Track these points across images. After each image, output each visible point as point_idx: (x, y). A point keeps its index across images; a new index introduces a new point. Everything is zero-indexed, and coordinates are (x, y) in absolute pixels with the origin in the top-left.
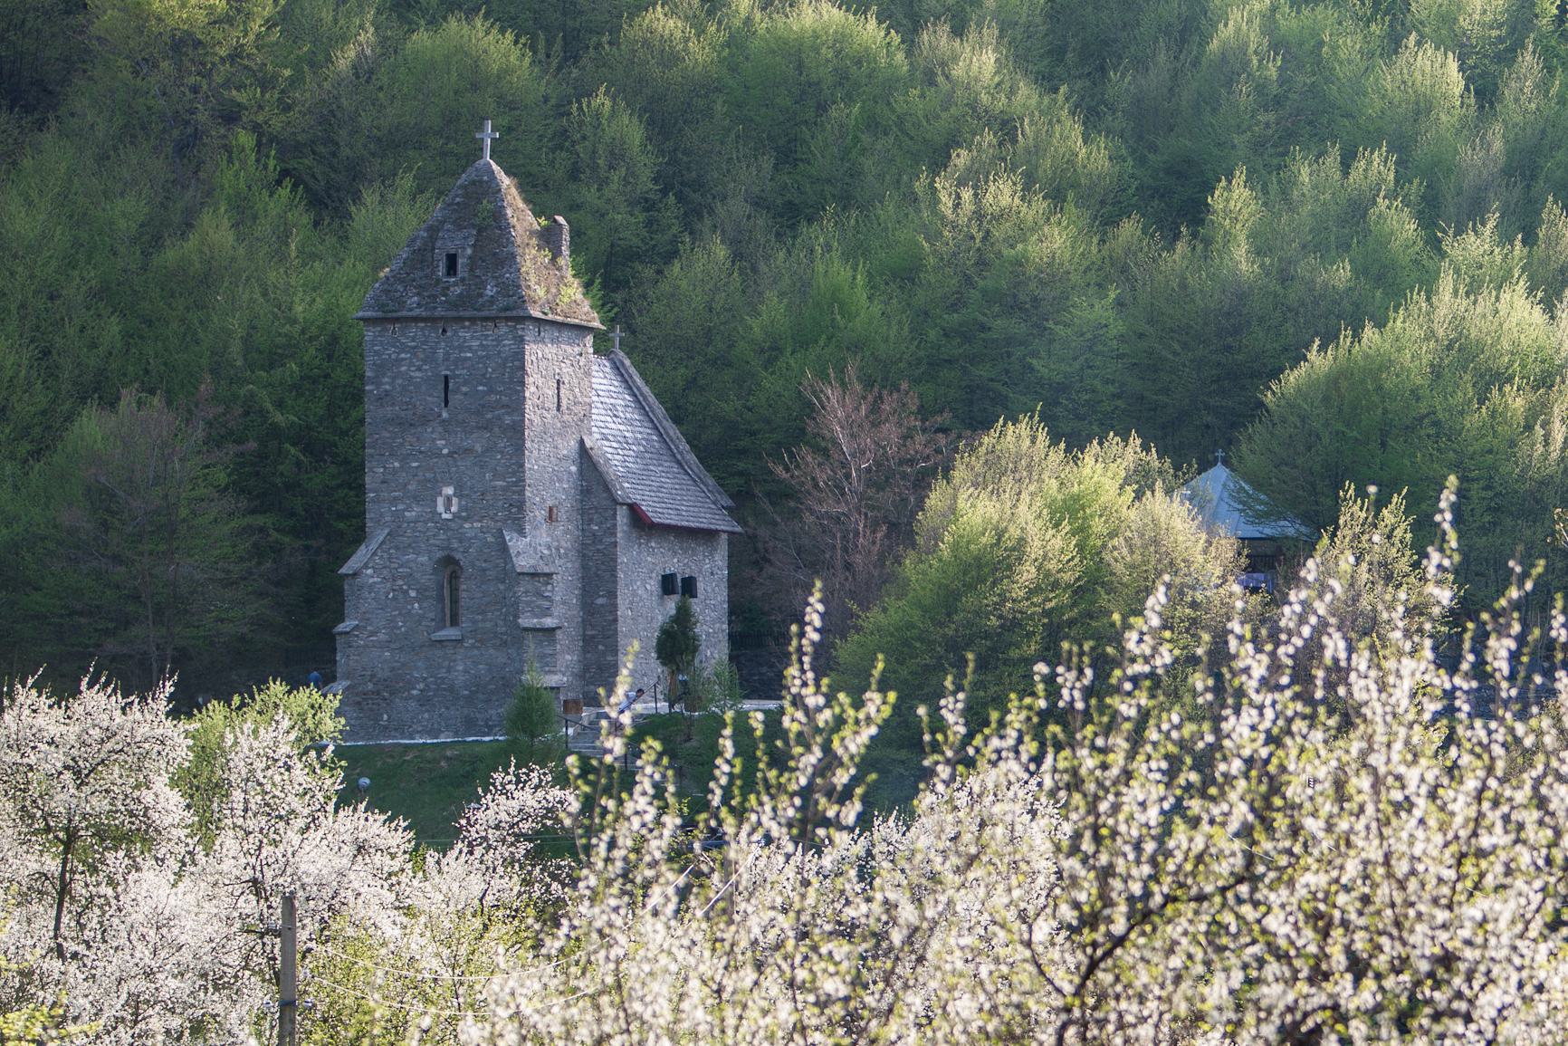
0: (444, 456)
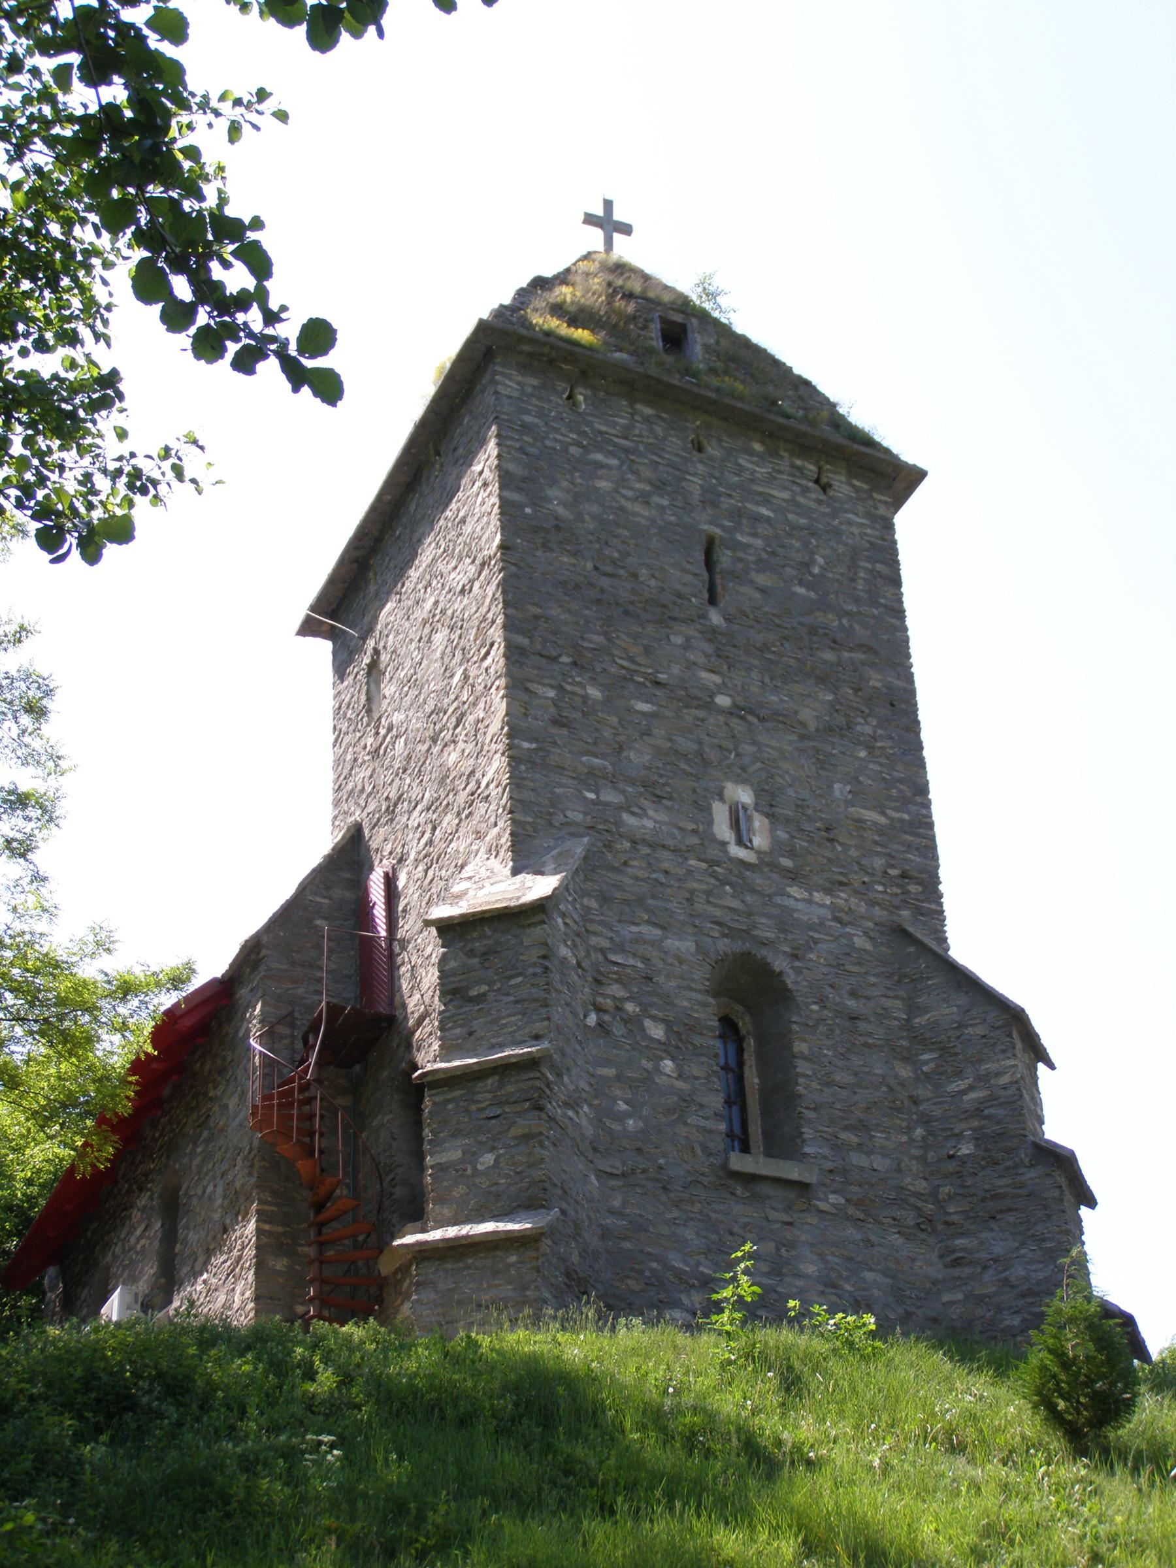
0: (722, 711)
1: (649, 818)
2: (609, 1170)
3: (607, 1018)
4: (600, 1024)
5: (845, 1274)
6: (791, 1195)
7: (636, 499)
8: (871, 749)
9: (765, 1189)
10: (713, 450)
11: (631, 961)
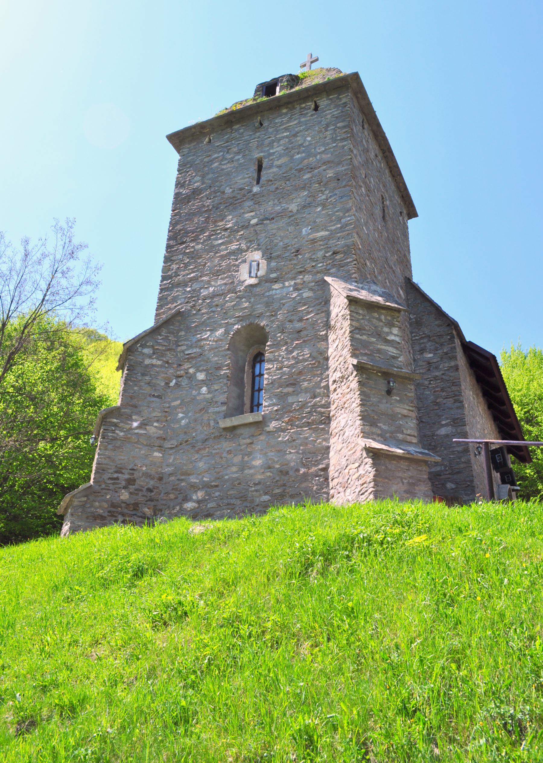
0: (254, 226)
1: (212, 286)
2: (170, 446)
3: (180, 379)
4: (176, 384)
5: (276, 459)
6: (252, 430)
7: (228, 162)
8: (324, 206)
9: (239, 431)
10: (265, 124)
11: (195, 351)
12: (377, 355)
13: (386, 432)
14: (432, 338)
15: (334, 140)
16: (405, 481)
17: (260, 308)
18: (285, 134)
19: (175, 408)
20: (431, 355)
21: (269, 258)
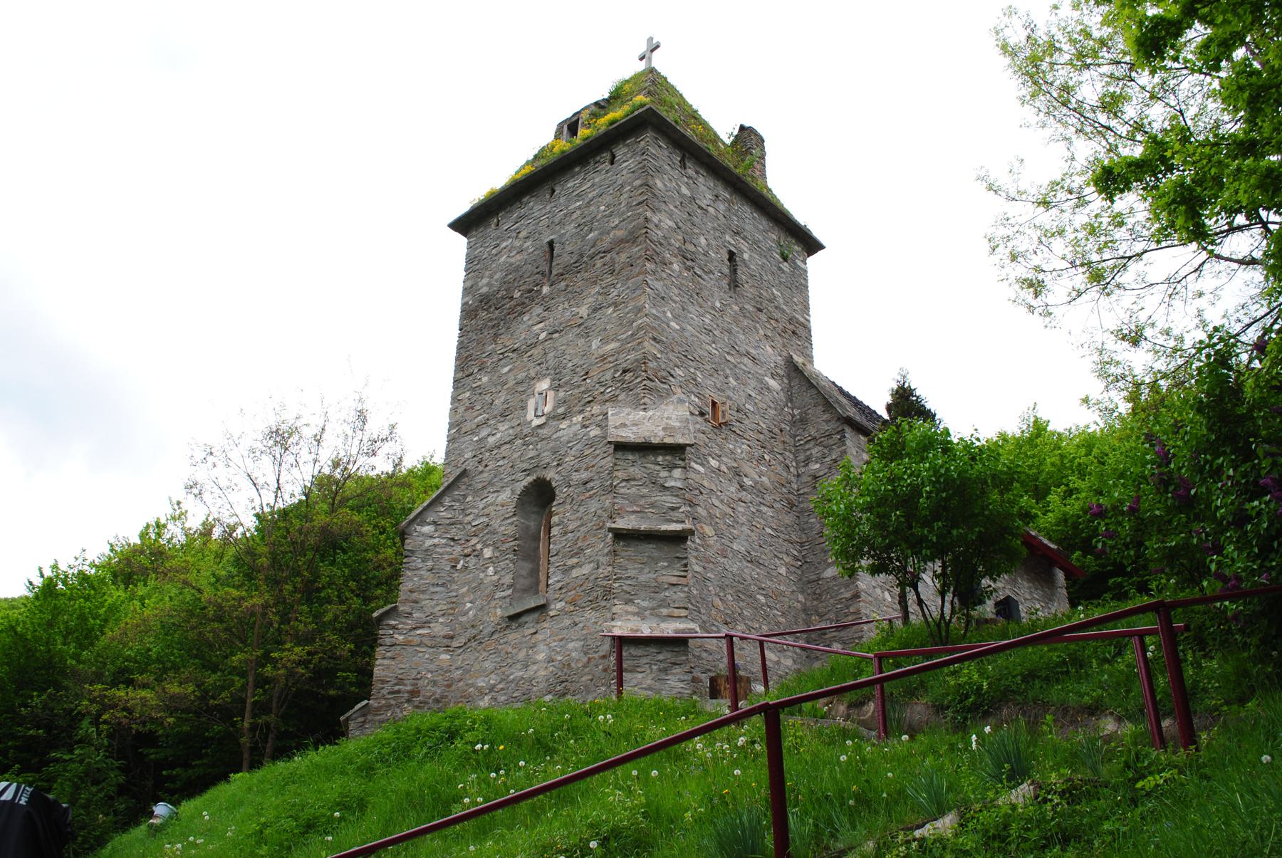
2: (458, 645)
3: (468, 559)
6: (536, 615)
12: (650, 510)
13: (645, 609)
14: (819, 441)
15: (629, 206)
16: (655, 667)
17: (546, 457)
18: (578, 204)
19: (463, 595)
20: (817, 466)
21: (556, 389)
